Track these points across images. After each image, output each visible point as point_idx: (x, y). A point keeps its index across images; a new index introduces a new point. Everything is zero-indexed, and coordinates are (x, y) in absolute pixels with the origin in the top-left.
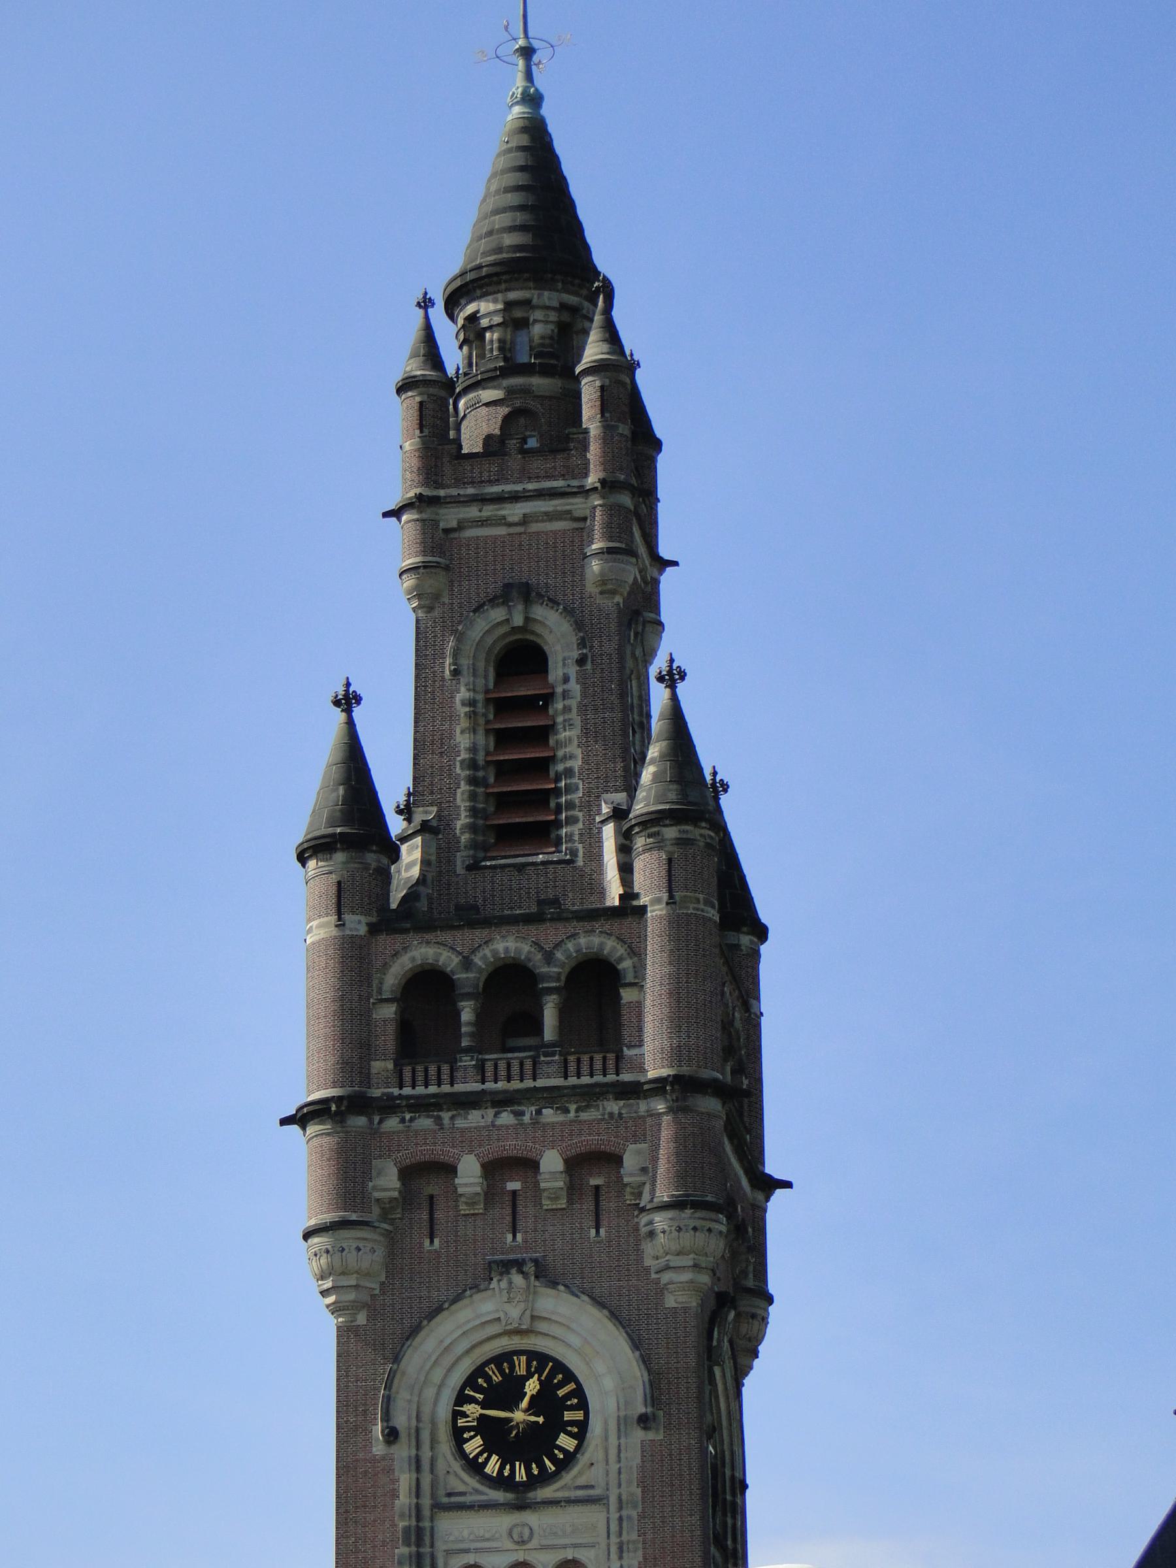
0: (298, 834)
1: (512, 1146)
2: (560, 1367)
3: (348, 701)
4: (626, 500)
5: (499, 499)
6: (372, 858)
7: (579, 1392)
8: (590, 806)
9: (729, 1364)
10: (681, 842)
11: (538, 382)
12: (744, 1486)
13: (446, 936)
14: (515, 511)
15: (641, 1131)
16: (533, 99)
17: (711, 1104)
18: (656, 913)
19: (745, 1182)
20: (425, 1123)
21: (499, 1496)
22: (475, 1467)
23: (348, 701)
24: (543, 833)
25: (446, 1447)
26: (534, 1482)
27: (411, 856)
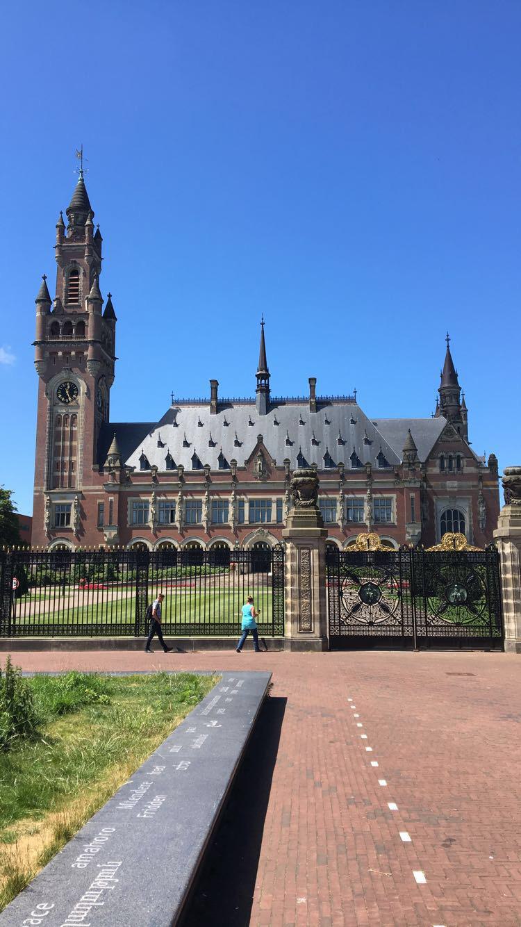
0: (36, 297)
3: (45, 278)
4: (92, 247)
6: (47, 303)
8: (83, 297)
11: (81, 228)
12: (108, 404)
14: (74, 248)
16: (82, 180)
17: (98, 345)
19: (110, 358)
20: (53, 346)
21: (61, 404)
22: (60, 399)
23: (45, 278)
24: (76, 301)
25: (56, 396)
26: (69, 402)
27: (55, 303)
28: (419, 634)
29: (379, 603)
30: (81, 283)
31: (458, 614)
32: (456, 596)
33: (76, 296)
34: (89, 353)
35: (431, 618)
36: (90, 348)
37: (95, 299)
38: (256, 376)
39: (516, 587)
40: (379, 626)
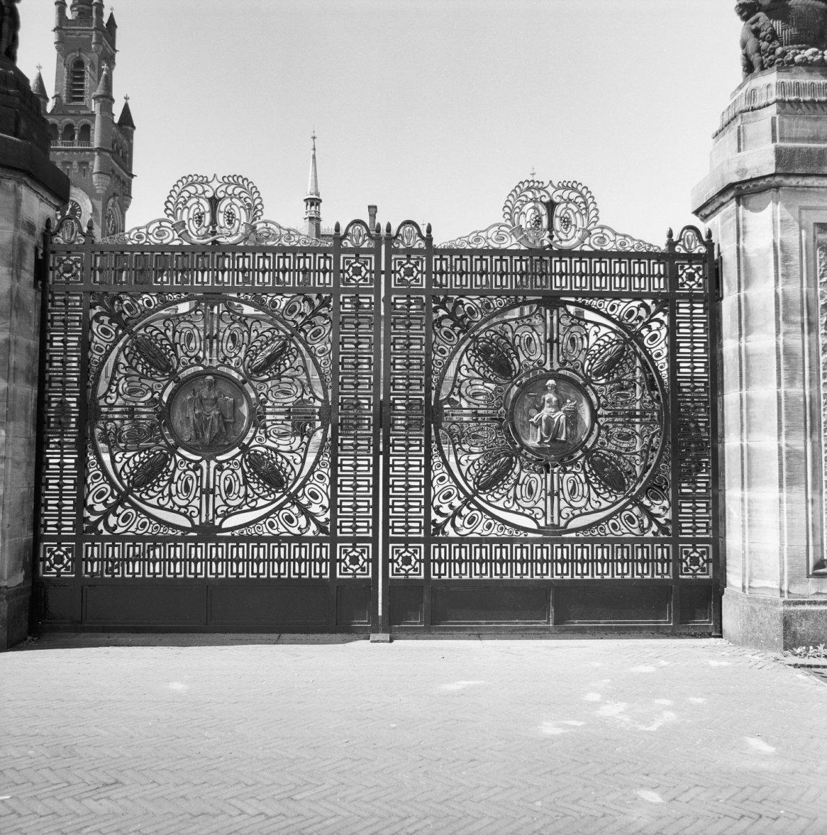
1: (65, 159)
2: (76, 203)
4: (100, 33)
5: (74, 30)
7: (80, 208)
8: (90, 94)
9: (118, 206)
10: (104, 102)
11: (85, 7)
13: (57, 117)
14: (78, 32)
15: (93, 160)
17: (108, 154)
18: (98, 115)
23: (39, 67)
24: (82, 99)
28: (397, 571)
29: (245, 449)
30: (87, 76)
31: (552, 494)
32: (549, 420)
33: (82, 93)
34: (96, 165)
35: (445, 509)
36: (97, 158)
37: (102, 96)
38: (306, 200)
39: (791, 381)
40: (238, 540)
